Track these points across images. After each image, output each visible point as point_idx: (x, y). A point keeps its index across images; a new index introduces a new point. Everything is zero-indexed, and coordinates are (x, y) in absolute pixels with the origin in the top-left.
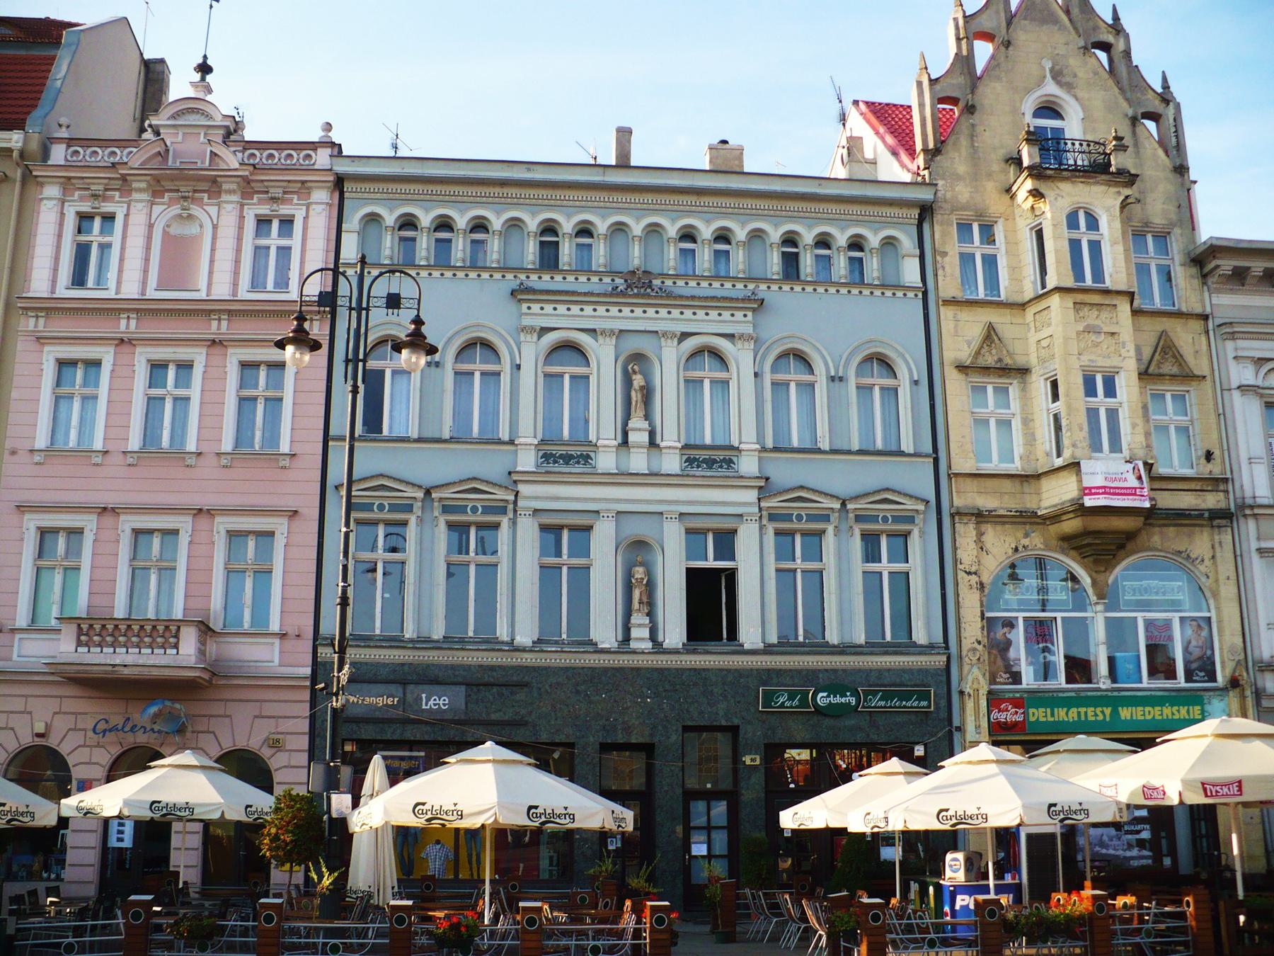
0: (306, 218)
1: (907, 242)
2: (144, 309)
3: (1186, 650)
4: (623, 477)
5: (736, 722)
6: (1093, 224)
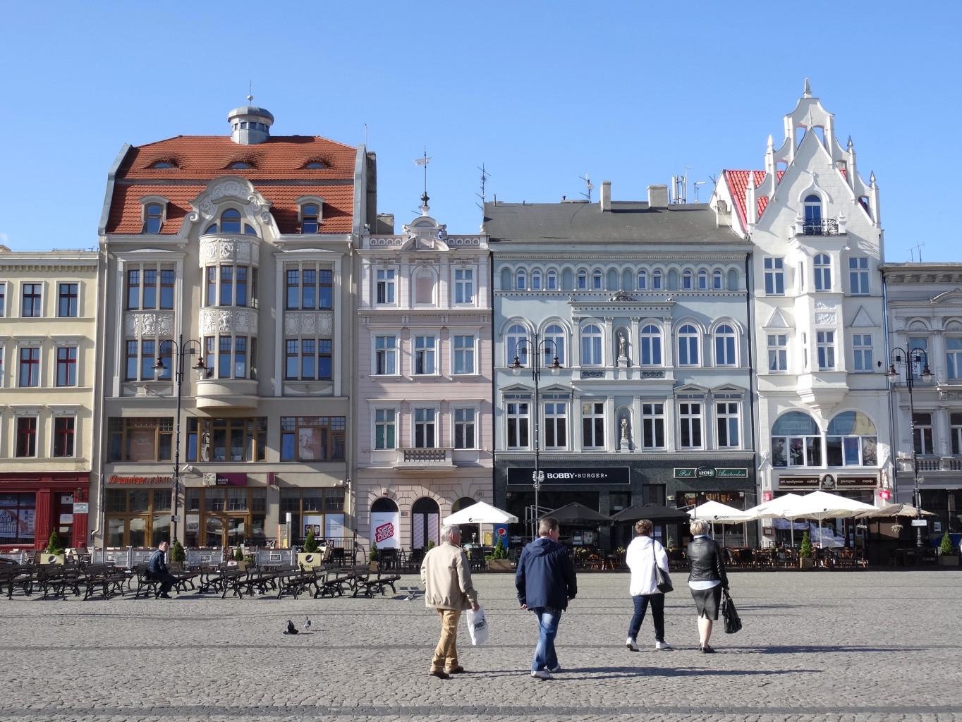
0: (478, 270)
1: (740, 270)
2: (411, 315)
3: (864, 452)
5: (665, 482)
6: (827, 260)
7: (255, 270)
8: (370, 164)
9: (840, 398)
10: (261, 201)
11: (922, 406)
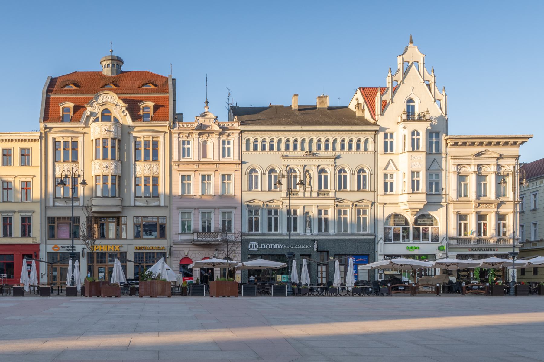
1: (371, 140)
4: (304, 198)
7: (119, 141)
8: (174, 80)
9: (421, 206)
10: (121, 104)
11: (463, 212)
